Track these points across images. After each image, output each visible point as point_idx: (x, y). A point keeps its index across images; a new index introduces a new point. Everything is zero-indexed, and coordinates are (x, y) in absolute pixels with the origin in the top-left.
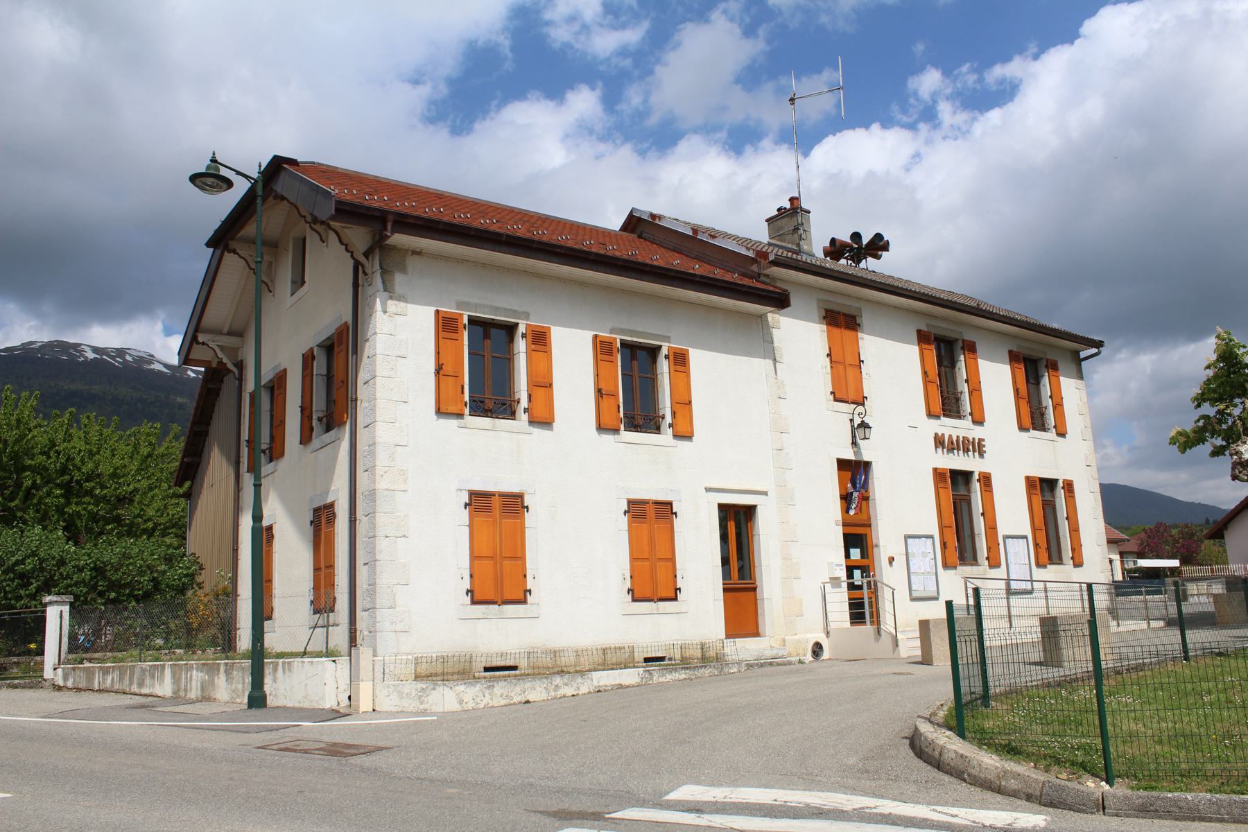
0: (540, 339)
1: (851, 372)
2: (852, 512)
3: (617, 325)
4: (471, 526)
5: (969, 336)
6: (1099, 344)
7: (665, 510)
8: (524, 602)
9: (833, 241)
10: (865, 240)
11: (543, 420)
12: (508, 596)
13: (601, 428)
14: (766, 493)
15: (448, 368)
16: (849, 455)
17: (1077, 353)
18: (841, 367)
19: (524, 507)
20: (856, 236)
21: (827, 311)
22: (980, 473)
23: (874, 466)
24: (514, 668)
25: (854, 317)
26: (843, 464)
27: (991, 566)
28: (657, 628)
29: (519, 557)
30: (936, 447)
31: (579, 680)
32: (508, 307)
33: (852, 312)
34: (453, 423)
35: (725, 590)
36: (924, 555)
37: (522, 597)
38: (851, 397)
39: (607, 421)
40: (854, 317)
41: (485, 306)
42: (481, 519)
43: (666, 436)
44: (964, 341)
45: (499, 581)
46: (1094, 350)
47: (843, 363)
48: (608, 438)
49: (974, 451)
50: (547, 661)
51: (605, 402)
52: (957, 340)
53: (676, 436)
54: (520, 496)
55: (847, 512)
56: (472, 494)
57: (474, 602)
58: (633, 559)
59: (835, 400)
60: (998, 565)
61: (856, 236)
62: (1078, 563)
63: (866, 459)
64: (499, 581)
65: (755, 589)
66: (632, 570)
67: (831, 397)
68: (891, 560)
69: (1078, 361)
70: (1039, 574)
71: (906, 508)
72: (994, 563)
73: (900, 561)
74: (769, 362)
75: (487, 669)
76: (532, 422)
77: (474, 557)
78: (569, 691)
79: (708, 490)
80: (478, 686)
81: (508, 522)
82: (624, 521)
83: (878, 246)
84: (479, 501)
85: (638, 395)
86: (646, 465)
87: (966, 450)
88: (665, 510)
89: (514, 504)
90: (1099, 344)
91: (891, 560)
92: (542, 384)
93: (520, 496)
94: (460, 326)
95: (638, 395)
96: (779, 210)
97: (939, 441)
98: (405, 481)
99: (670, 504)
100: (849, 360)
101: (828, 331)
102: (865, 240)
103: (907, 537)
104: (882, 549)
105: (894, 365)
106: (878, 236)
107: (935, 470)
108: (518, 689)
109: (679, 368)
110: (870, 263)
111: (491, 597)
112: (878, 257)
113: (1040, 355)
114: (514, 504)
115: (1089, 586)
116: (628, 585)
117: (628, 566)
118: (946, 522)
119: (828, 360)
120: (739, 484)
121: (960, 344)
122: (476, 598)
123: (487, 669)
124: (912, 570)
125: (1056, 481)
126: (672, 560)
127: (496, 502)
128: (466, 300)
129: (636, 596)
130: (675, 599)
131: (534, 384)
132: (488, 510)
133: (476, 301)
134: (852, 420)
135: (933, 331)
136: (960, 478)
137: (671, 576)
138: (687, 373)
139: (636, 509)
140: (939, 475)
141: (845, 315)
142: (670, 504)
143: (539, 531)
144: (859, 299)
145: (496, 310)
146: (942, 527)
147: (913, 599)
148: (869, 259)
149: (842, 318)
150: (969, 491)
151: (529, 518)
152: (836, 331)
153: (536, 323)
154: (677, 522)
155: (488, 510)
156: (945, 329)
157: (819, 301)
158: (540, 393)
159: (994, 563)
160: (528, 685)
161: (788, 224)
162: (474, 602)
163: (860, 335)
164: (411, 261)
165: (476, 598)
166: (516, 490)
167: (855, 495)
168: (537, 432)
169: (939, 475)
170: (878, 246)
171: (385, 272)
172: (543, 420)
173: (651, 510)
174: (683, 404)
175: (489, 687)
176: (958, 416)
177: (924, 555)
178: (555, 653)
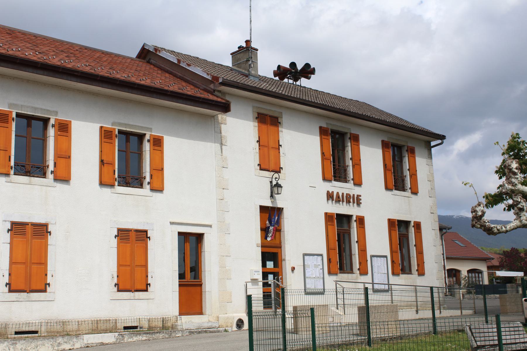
0: (64, 128)
1: (272, 153)
2: (269, 239)
3: (116, 121)
4: (11, 244)
6: (442, 138)
7: (142, 235)
8: (45, 291)
9: (279, 67)
10: (299, 67)
11: (63, 177)
12: (34, 287)
13: (102, 184)
14: (210, 226)
16: (268, 203)
17: (429, 142)
18: (266, 149)
19: (48, 232)
20: (293, 65)
22: (357, 216)
23: (285, 211)
24: (36, 332)
25: (277, 118)
26: (263, 209)
27: (361, 274)
28: (134, 308)
29: (43, 263)
30: (328, 200)
31: (75, 340)
32: (44, 107)
33: (275, 115)
35: (180, 285)
36: (316, 266)
38: (272, 167)
39: (105, 180)
40: (277, 118)
41: (28, 107)
42: (18, 239)
43: (146, 190)
44: (351, 134)
45: (28, 278)
46: (439, 141)
47: (268, 147)
48: (107, 191)
49: (354, 202)
50: (59, 328)
51: (106, 168)
52: (346, 133)
53: (152, 190)
54: (46, 225)
55: (266, 238)
56: (13, 224)
57: (10, 291)
58: (120, 265)
59: (261, 169)
60: (366, 273)
61: (293, 65)
62: (421, 273)
63: (279, 205)
64: (28, 278)
65: (201, 285)
67: (258, 168)
68: (293, 269)
69: (429, 148)
70: (394, 280)
71: (305, 237)
72: (363, 272)
73: (299, 270)
74: (218, 145)
75: (17, 333)
76: (56, 179)
77: (12, 263)
78: (67, 347)
79: (172, 223)
80: (6, 343)
81: (36, 241)
82: (115, 242)
83: (308, 71)
85: (129, 163)
86: (131, 207)
87: (348, 202)
88: (142, 235)
89: (41, 230)
90: (442, 138)
91: (293, 269)
92: (64, 156)
93: (46, 225)
94: (10, 119)
95: (129, 163)
96: (239, 48)
97: (330, 196)
99: (146, 232)
100: (272, 144)
101: (259, 127)
102: (299, 67)
103: (305, 255)
104: (287, 261)
105: (302, 146)
106: (307, 65)
107: (326, 214)
108: (33, 345)
109: (156, 148)
110: (303, 82)
111: (22, 287)
112: (309, 78)
113: (403, 143)
114: (41, 230)
115: (432, 288)
116: (115, 281)
117: (115, 269)
118: (331, 246)
119: (257, 144)
120: (193, 219)
121: (349, 136)
122: (12, 288)
123: (17, 333)
124: (307, 276)
125: (410, 222)
126: (145, 266)
127: (29, 229)
128: (15, 102)
129: (120, 288)
130: (146, 290)
131: (58, 156)
132: (24, 234)
133: (23, 104)
134: (271, 182)
135: (330, 127)
136: (343, 220)
137: (144, 276)
138: (162, 152)
139: (123, 235)
140: (329, 217)
141: (271, 117)
142: (146, 232)
144: (281, 106)
145: (36, 109)
146: (329, 249)
147: (307, 293)
148: (303, 79)
150: (349, 227)
151: (51, 239)
152: (264, 127)
153: (62, 117)
154: (150, 243)
155: (24, 234)
156: (339, 126)
157: (253, 107)
158: (62, 161)
159: (363, 272)
160: (40, 342)
161: (243, 57)
162: (10, 291)
163: (280, 129)
165: (12, 288)
166: (43, 221)
167: (271, 228)
168: (60, 186)
169: (329, 217)
170: (308, 71)
172: (63, 177)
173: (133, 235)
174: (158, 170)
175: (13, 344)
176: (346, 181)
177: (316, 266)
178: (64, 323)
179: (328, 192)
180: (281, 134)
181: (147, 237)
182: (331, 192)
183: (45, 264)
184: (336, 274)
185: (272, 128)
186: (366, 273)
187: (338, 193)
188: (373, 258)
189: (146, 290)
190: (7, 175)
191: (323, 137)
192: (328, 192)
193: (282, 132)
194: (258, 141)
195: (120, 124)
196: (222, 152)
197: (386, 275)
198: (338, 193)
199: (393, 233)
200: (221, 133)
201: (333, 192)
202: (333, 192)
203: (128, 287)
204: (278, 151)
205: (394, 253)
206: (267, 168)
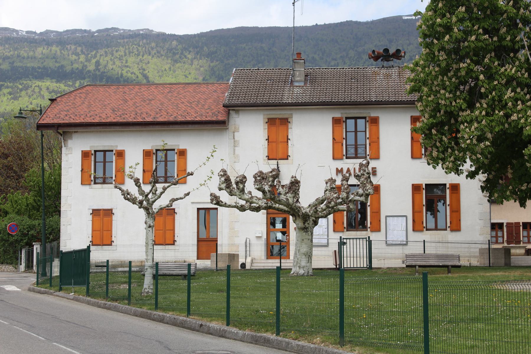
0: (121, 154)
3: (155, 144)
4: (92, 221)
5: (373, 114)
8: (111, 245)
12: (105, 243)
15: (86, 170)
18: (274, 144)
20: (386, 50)
21: (269, 119)
25: (287, 119)
34: (87, 187)
37: (110, 243)
38: (280, 156)
40: (287, 119)
42: (96, 218)
54: (111, 210)
56: (93, 210)
59: (269, 159)
60: (379, 230)
61: (386, 50)
66: (92, 234)
67: (266, 158)
72: (377, 229)
77: (93, 231)
79: (193, 203)
81: (106, 219)
84: (95, 213)
89: (109, 213)
93: (111, 210)
94: (90, 155)
95: (164, 169)
98: (71, 207)
100: (280, 139)
101: (268, 128)
111: (99, 243)
114: (109, 213)
119: (267, 142)
125: (445, 185)
126: (174, 230)
130: (174, 244)
131: (117, 171)
132: (99, 215)
137: (172, 236)
138: (186, 159)
141: (279, 119)
143: (117, 222)
145: (105, 146)
149: (278, 121)
151: (114, 217)
152: (274, 129)
153: (120, 148)
155: (99, 215)
157: (264, 115)
164: (75, 136)
166: (109, 208)
171: (65, 140)
179: (337, 169)
180: (290, 130)
181: (175, 213)
182: (339, 169)
183: (111, 230)
184: (343, 231)
185: (282, 128)
186: (379, 230)
187: (348, 169)
188: (388, 218)
189: (174, 244)
190: (90, 184)
191: (335, 125)
192: (337, 169)
193: (291, 128)
194: (268, 140)
195: (157, 146)
196: (234, 152)
197: (405, 232)
198: (348, 169)
199: (417, 196)
200: (234, 138)
201: (342, 168)
202: (342, 168)
203: (161, 243)
204: (286, 144)
205: (416, 214)
206: (275, 157)
